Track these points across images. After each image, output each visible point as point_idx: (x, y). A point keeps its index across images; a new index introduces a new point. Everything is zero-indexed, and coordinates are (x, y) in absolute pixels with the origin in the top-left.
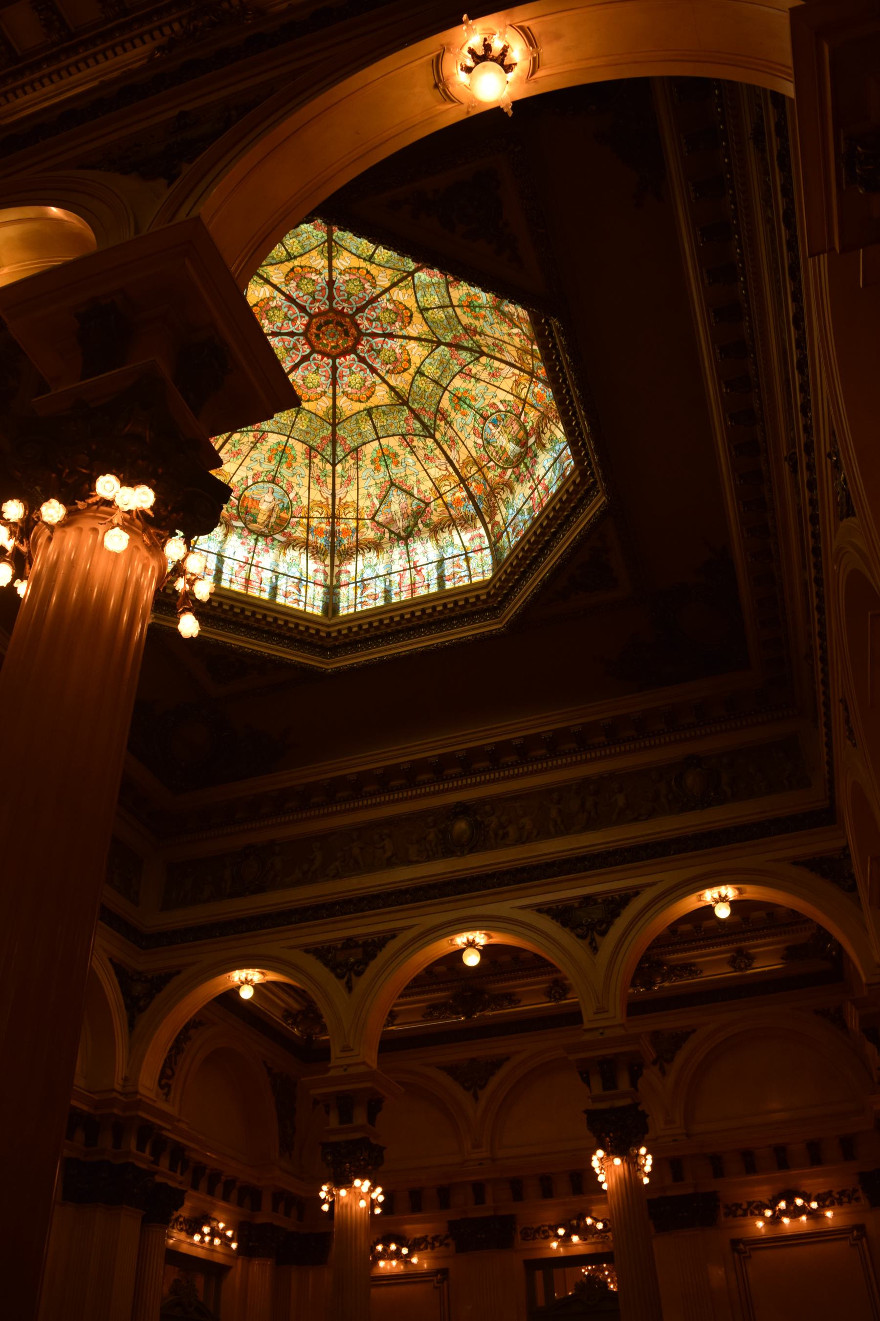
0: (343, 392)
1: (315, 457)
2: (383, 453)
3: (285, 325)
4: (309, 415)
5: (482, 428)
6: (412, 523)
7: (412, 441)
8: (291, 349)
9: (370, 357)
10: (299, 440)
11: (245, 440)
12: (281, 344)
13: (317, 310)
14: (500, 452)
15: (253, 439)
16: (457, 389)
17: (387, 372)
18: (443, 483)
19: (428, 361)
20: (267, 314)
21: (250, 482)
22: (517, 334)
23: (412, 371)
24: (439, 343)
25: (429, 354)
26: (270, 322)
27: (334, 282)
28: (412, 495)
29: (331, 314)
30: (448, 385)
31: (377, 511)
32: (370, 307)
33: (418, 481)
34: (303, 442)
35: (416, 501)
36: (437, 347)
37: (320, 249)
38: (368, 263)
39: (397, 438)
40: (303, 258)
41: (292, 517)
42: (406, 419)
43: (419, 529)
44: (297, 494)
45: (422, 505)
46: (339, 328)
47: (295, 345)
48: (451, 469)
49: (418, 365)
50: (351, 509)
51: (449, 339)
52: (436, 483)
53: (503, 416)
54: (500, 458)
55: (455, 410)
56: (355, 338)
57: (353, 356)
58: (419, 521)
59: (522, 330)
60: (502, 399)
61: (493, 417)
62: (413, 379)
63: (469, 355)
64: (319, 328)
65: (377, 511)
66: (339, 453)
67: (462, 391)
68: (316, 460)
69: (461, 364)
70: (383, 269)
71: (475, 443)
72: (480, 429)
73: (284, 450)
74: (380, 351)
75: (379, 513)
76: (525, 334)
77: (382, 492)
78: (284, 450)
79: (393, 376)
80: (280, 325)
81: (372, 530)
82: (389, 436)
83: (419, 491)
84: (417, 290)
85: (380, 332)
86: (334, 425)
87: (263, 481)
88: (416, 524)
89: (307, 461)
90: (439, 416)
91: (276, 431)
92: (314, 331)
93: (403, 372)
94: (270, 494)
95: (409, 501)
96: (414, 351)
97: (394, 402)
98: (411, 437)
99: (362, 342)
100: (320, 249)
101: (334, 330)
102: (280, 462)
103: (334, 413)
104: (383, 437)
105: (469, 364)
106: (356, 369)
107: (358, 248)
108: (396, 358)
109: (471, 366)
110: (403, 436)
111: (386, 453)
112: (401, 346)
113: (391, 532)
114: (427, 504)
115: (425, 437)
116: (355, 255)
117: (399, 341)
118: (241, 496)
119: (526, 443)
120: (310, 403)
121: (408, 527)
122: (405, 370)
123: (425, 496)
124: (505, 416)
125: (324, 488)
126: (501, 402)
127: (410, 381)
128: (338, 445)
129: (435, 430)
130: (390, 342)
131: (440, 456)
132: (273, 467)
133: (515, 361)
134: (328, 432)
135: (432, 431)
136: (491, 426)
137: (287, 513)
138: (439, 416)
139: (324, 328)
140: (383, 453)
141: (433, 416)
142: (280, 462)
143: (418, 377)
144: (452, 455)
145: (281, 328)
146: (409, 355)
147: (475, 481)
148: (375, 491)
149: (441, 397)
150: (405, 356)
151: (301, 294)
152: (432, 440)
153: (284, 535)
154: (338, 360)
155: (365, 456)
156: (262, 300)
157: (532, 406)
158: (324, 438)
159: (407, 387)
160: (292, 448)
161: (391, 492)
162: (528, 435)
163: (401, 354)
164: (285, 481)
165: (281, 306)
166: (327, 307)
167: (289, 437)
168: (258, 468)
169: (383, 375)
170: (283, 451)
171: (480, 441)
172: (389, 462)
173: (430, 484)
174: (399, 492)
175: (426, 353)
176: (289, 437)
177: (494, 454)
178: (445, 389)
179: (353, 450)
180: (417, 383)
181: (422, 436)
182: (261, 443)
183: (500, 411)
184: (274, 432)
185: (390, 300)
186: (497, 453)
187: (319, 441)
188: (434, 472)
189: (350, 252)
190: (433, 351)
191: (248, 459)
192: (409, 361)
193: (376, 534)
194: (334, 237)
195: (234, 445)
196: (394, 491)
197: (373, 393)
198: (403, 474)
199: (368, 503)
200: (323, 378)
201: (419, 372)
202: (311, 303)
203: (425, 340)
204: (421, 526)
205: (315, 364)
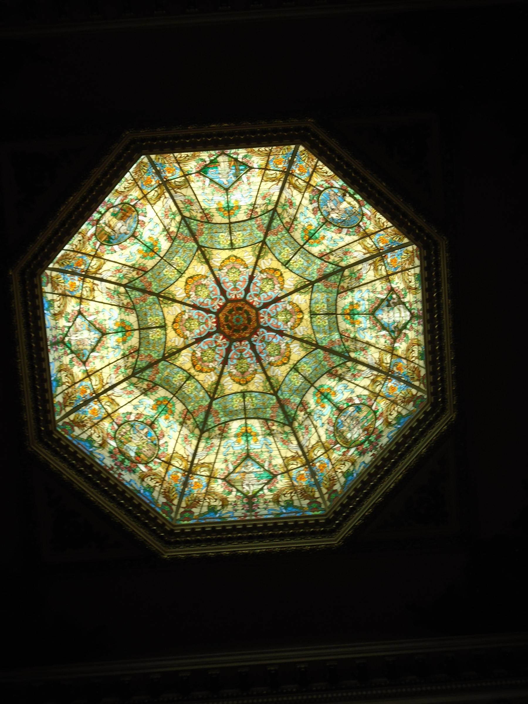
0: (185, 311)
1: (137, 274)
2: (128, 331)
3: (257, 288)
4: (174, 279)
5: (142, 422)
6: (73, 348)
7: (133, 357)
8: (235, 285)
9: (211, 342)
10: (156, 265)
11: (173, 224)
12: (241, 279)
13: (262, 316)
14: (127, 436)
15: (171, 230)
16: (174, 405)
17: (194, 351)
18: (98, 379)
19: (199, 386)
20: (270, 279)
21: (141, 218)
22: (227, 467)
23: (192, 371)
24: (213, 399)
25: (204, 389)
26: (263, 279)
27: (282, 336)
28: (93, 350)
29: (256, 325)
30: (177, 398)
31: (84, 317)
32: (253, 354)
33: (103, 358)
34: (153, 267)
35: (88, 353)
36: (209, 396)
37: (313, 336)
38: (292, 366)
39: (137, 345)
40: (309, 323)
41: (102, 244)
42: (151, 356)
43: (68, 355)
44: (115, 252)
45: (85, 359)
46: (243, 327)
47: (237, 289)
48: (107, 387)
49: (196, 377)
50: (89, 293)
51: (215, 406)
52: (98, 373)
53: (155, 442)
54: (122, 436)
55: (156, 400)
56: (230, 336)
57: (215, 329)
58: (74, 355)
59: (232, 473)
60: (169, 444)
61: (153, 433)
62: (184, 370)
63: (201, 420)
64: (246, 312)
65: (84, 317)
66: (134, 293)
67: (173, 409)
68: (134, 273)
69: (194, 412)
70: (284, 375)
71: (131, 413)
72: (141, 420)
73: (153, 251)
74: (214, 350)
75: (83, 319)
76: (229, 474)
77: (98, 324)
78: (153, 251)
79: (190, 355)
80: (258, 285)
81: (73, 311)
82: (140, 339)
83: (95, 357)
84: (262, 394)
85: (230, 356)
86: (158, 295)
87: (136, 228)
88: (72, 352)
89: (137, 266)
90: (151, 385)
91: (171, 250)
92: (246, 308)
93: (193, 364)
94: (125, 231)
95: (89, 348)
96: (209, 377)
97: (167, 349)
98: (136, 357)
99: (224, 340)
100: (313, 336)
101: (241, 323)
102: (145, 245)
103: (169, 299)
104: (140, 334)
105: (194, 419)
106: (203, 328)
107: (307, 363)
108: (205, 361)
109: (192, 420)
110: (138, 351)
111: (127, 334)
112: (215, 368)
113: (70, 328)
114: (84, 363)
115: (134, 368)
116: (301, 359)
117: (219, 368)
118: (135, 208)
119: (140, 463)
120: (184, 284)
121: (71, 344)
122: (194, 366)
123: (91, 362)
124: (155, 445)
125: (110, 273)
126: (166, 442)
127: (183, 367)
128: (141, 294)
129: (139, 378)
130: (221, 360)
131: (117, 379)
132: (143, 239)
133: (199, 460)
134: (154, 288)
135: (137, 375)
136: (146, 430)
137: (104, 241)
138: (151, 385)
139: (245, 316)
140: (128, 331)
141: (151, 379)
142: (145, 245)
143: (185, 374)
144: (118, 389)
145: (255, 284)
146: (206, 372)
147: (100, 409)
148: (100, 317)
149: (167, 390)
150: (205, 369)
151: (278, 309)
152: (130, 374)
153: (92, 235)
154: (214, 316)
155: (128, 315)
156: (283, 281)
157: (167, 470)
158: (150, 284)
159: (178, 363)
160: (152, 258)
161: (97, 332)
162: (146, 464)
163: (208, 366)
164: (129, 245)
165: (273, 291)
166: (262, 324)
167: (162, 258)
168: (149, 226)
169: (193, 347)
170: (152, 251)
171: (132, 418)
172: (120, 334)
173: (98, 368)
174: (96, 339)
175: (206, 386)
176: (162, 258)
177: (124, 430)
178: (174, 395)
179: (134, 306)
180: (181, 372)
181: (135, 367)
182: (166, 235)
183: (159, 440)
184: (170, 247)
185: (255, 372)
186: (125, 433)
187: (149, 280)
188: (106, 373)
189: (304, 357)
190: (207, 392)
191: (159, 222)
192: (201, 371)
193: (69, 314)
194: (319, 350)
195: (173, 214)
196: (97, 335)
197: (178, 335)
198: (108, 345)
199: (92, 310)
200: (202, 301)
201: (190, 377)
202: (269, 314)
203: (216, 389)
204: (70, 356)
205: (216, 298)
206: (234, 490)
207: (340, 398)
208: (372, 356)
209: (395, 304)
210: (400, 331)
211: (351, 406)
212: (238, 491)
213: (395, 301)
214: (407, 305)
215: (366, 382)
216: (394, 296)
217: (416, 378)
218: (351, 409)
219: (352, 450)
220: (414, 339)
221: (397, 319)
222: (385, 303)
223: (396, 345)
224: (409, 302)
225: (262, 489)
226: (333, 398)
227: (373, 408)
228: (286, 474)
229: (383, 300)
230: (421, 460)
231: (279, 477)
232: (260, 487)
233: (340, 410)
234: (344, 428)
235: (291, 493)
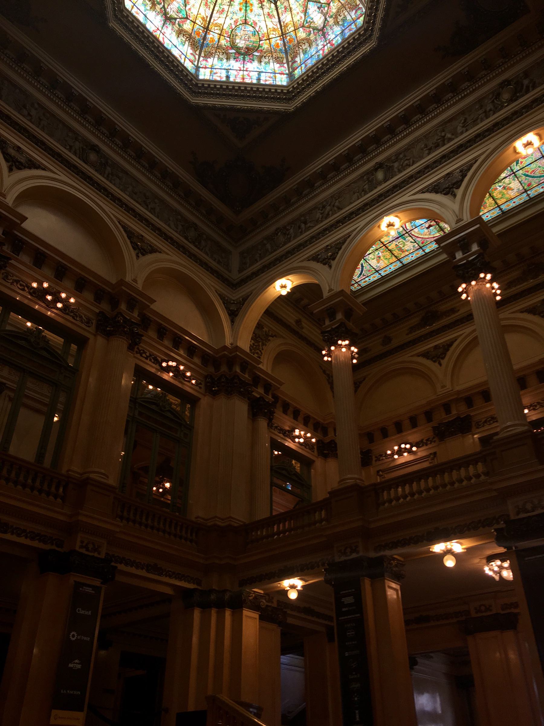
206: (163, 4)
207: (252, 17)
208: (286, 18)
209: (322, 12)
210: (309, 27)
211: (253, 27)
212: (164, 6)
213: (324, 11)
214: (326, 22)
215: (270, 25)
216: (326, 9)
217: (292, 56)
218: (251, 29)
219: (233, 51)
220: (311, 40)
221: (315, 20)
222: (319, 5)
223: (301, 29)
224: (328, 22)
225: (176, 19)
226: (249, 11)
227: (261, 42)
228: (193, 23)
229: (320, 2)
230: (260, 111)
231: (188, 21)
232: (176, 16)
233: (246, 22)
234: (239, 34)
235: (187, 38)
